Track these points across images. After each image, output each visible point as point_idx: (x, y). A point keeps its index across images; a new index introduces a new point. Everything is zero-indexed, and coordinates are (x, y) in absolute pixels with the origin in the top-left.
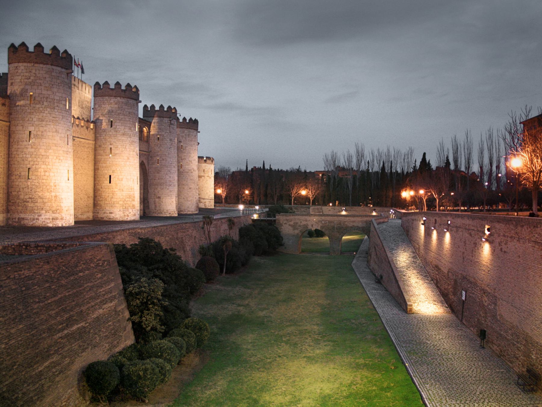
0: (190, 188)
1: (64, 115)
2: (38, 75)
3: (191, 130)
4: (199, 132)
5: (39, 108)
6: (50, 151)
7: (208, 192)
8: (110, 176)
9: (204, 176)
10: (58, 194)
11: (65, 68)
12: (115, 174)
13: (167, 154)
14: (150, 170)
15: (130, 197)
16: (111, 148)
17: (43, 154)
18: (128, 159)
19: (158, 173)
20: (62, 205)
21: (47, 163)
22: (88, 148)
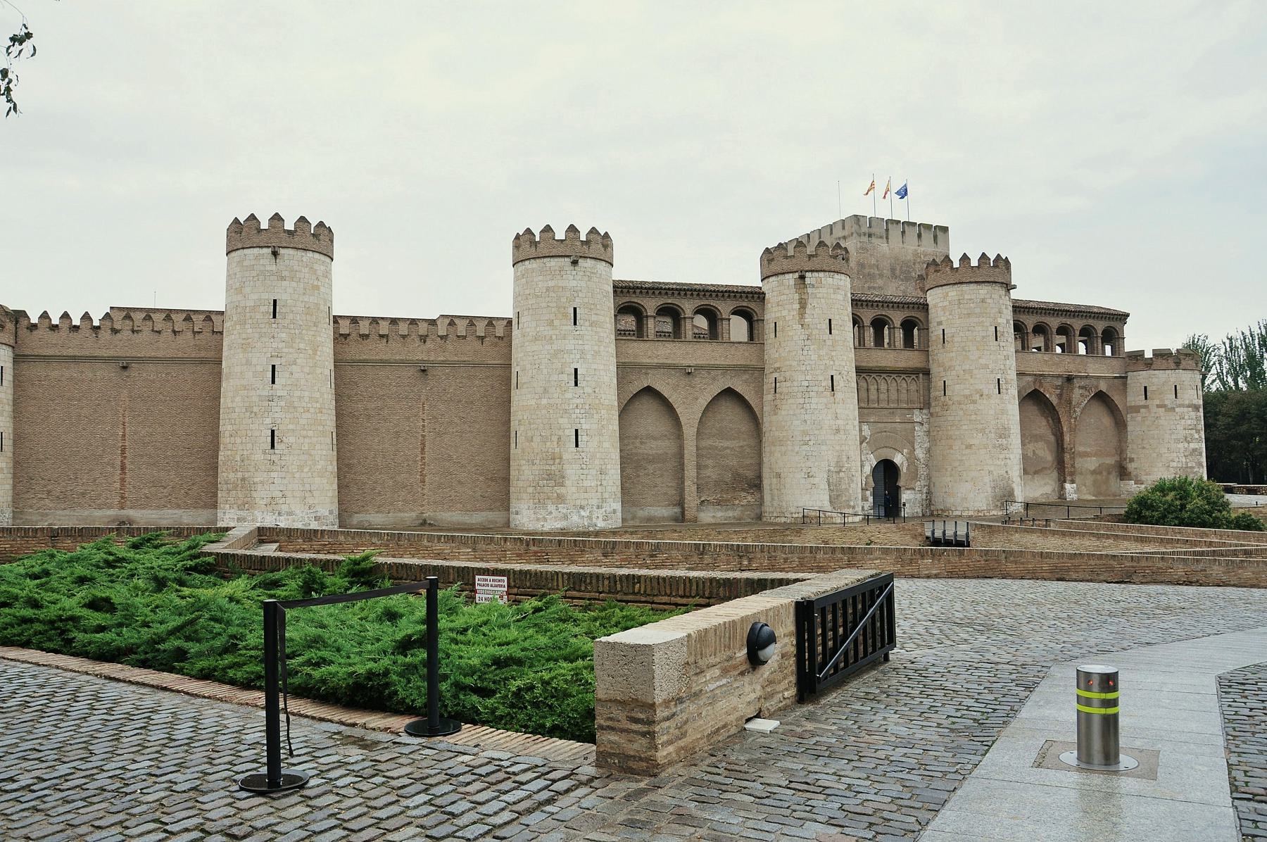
0: (969, 447)
3: (965, 287)
4: (1014, 287)
9: (1146, 407)
10: (247, 475)
13: (794, 364)
15: (550, 476)
20: (254, 494)
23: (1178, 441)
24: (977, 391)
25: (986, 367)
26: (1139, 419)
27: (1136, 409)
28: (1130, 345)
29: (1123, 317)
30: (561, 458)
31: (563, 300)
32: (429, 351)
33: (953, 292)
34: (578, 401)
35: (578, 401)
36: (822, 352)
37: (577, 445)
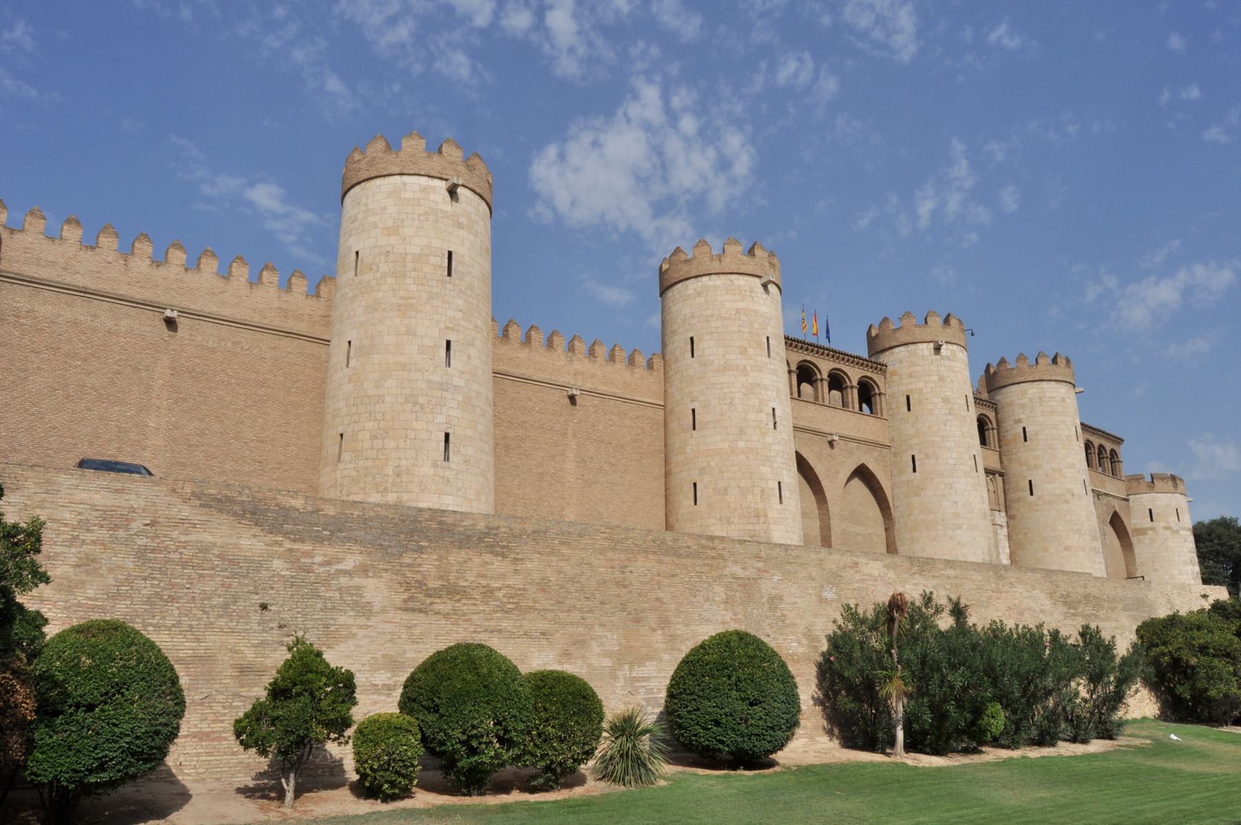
0: (1067, 548)
1: (434, 290)
2: (371, 206)
5: (369, 282)
6: (387, 384)
7: (1175, 572)
8: (695, 485)
9: (1153, 529)
11: (441, 179)
12: (707, 478)
14: (896, 491)
16: (693, 411)
17: (370, 392)
18: (742, 431)
19: (917, 495)
21: (379, 416)
22: (637, 417)
23: (1185, 563)
24: (1069, 491)
25: (1072, 466)
26: (1147, 541)
27: (1142, 532)
28: (1126, 469)
29: (1119, 441)
30: (766, 516)
31: (756, 325)
32: (576, 374)
33: (1032, 390)
34: (778, 447)
35: (778, 447)
36: (965, 429)
37: (781, 502)
